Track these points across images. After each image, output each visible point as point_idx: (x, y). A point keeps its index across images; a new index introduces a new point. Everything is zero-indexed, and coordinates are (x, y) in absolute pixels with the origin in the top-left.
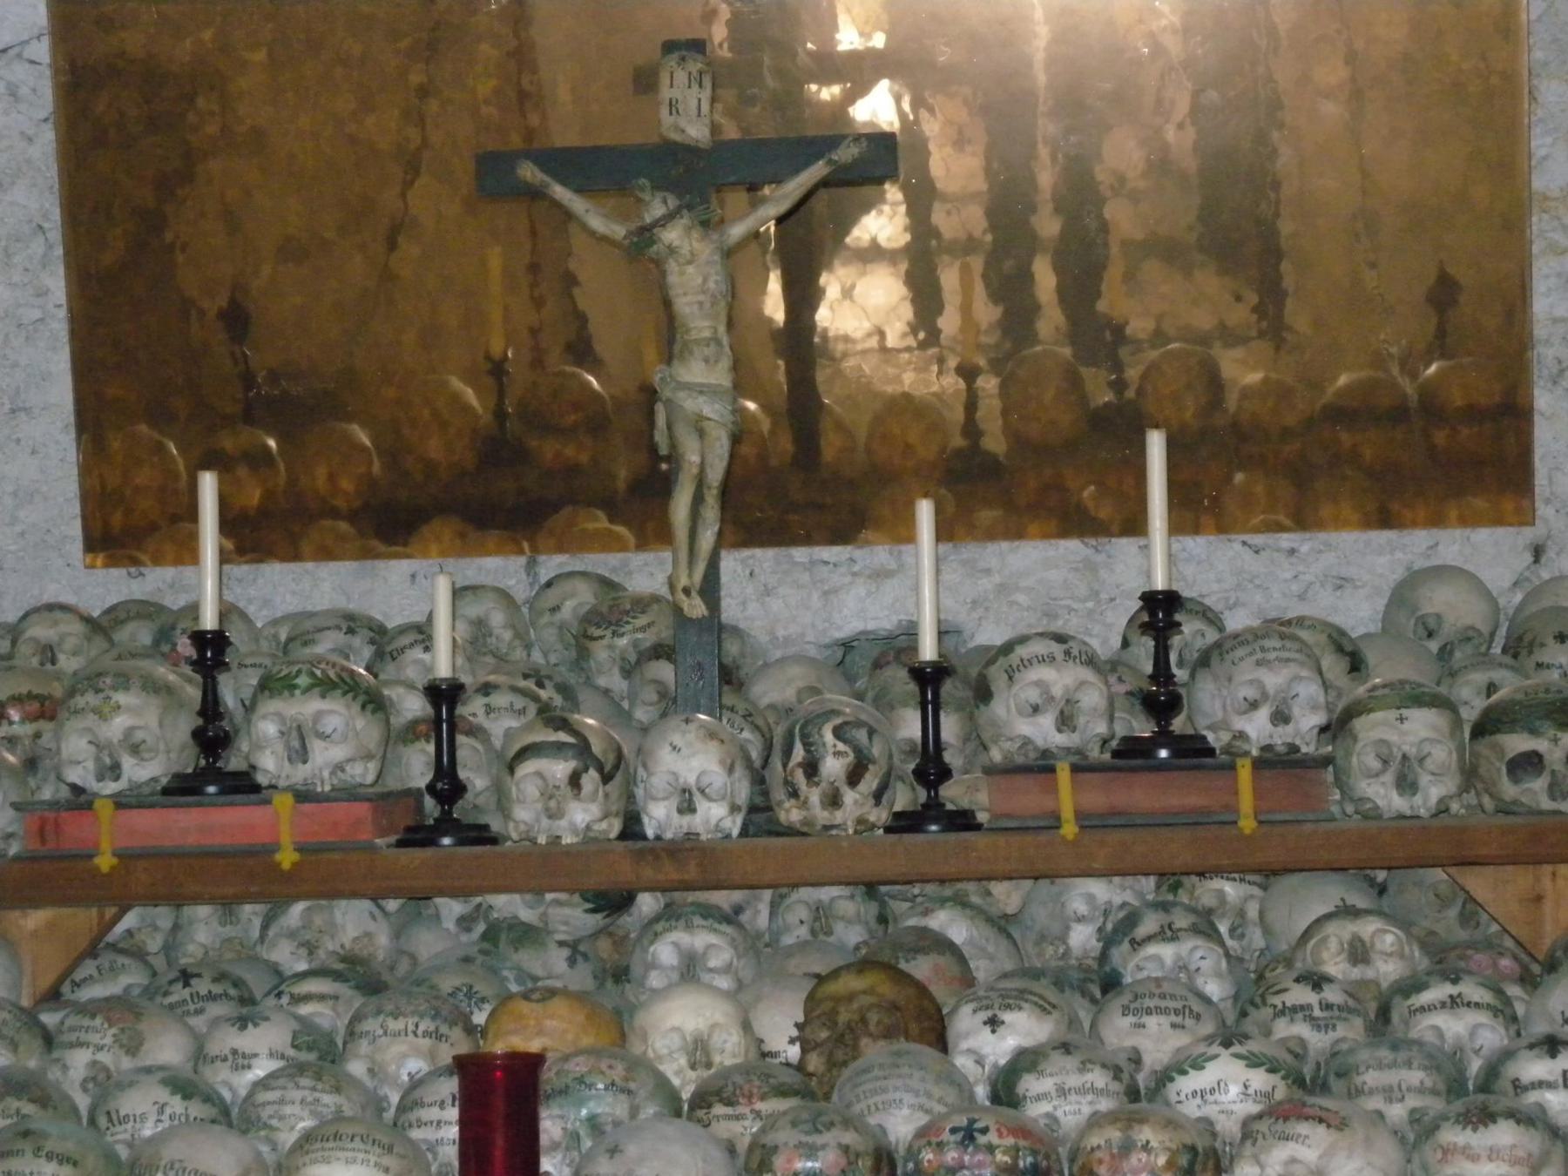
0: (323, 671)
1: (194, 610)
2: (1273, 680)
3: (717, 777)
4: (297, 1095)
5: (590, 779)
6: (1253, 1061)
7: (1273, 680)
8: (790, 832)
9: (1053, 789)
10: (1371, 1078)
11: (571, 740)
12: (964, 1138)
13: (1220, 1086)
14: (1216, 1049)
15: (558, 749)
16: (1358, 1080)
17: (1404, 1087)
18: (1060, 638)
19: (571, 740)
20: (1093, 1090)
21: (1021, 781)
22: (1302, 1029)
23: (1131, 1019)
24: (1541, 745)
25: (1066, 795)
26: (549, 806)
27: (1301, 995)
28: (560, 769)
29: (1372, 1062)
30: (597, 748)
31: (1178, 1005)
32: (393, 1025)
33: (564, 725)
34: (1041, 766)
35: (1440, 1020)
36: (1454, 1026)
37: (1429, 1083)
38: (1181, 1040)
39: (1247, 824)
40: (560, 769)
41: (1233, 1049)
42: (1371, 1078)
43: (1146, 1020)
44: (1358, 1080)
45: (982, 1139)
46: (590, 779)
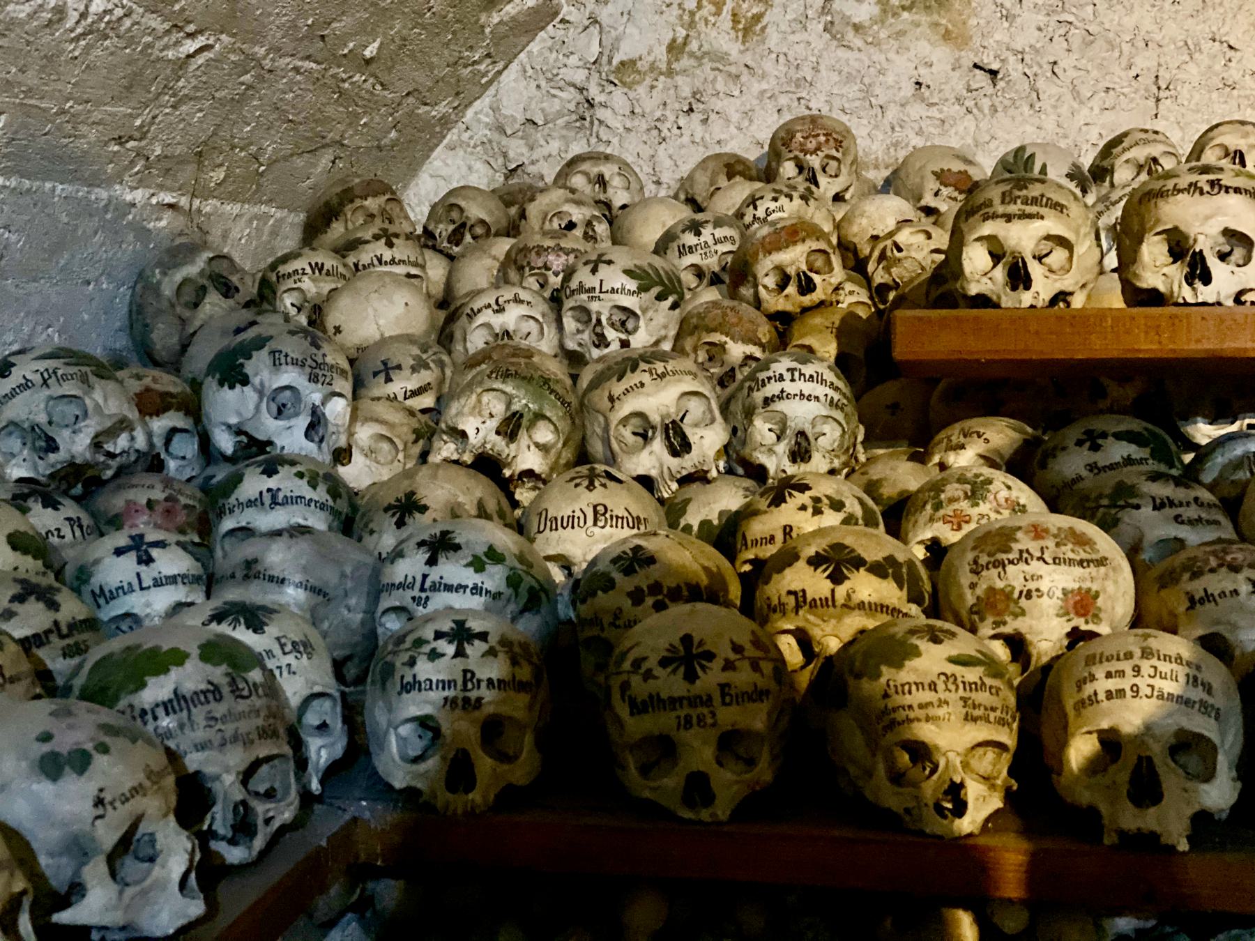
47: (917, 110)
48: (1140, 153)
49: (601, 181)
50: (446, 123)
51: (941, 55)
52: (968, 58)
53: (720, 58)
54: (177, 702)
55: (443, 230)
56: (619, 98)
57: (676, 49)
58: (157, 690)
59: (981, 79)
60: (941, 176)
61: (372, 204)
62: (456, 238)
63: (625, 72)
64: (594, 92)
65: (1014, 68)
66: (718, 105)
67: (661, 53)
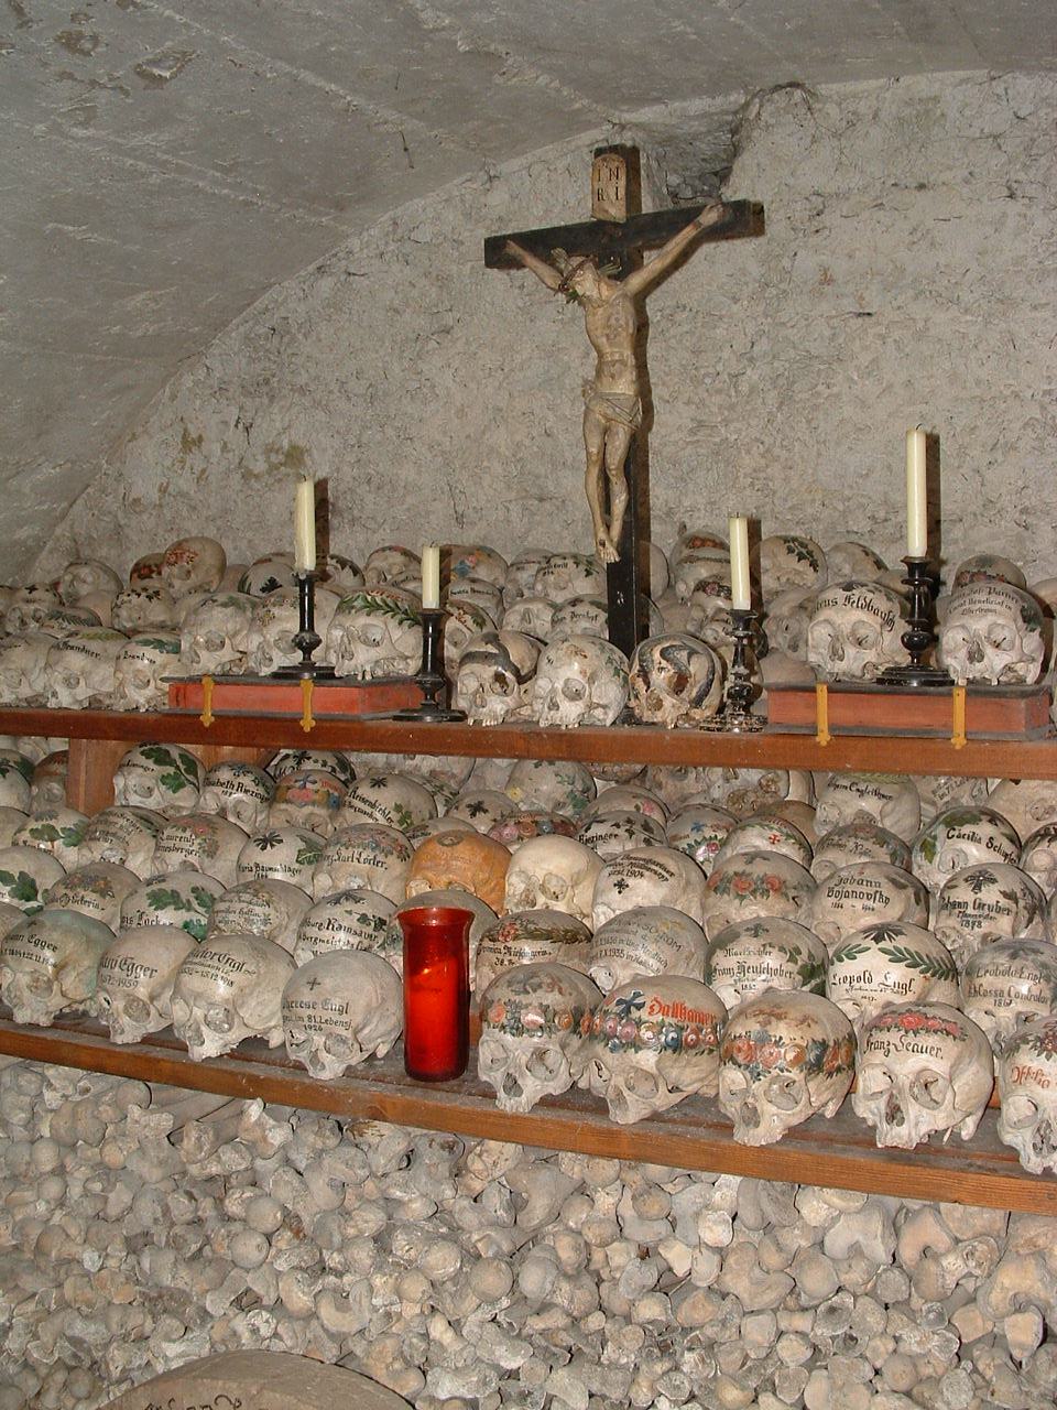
0: (373, 597)
1: (287, 557)
4: (237, 906)
6: (896, 957)
9: (814, 706)
10: (987, 981)
11: (495, 651)
12: (622, 1011)
13: (866, 977)
14: (869, 943)
16: (978, 981)
17: (1012, 994)
19: (495, 651)
20: (768, 970)
21: (790, 697)
23: (833, 900)
25: (823, 711)
29: (990, 968)
31: (871, 890)
32: (345, 853)
37: (1036, 992)
39: (959, 741)
41: (882, 945)
42: (987, 981)
43: (844, 901)
44: (978, 981)
45: (635, 1014)
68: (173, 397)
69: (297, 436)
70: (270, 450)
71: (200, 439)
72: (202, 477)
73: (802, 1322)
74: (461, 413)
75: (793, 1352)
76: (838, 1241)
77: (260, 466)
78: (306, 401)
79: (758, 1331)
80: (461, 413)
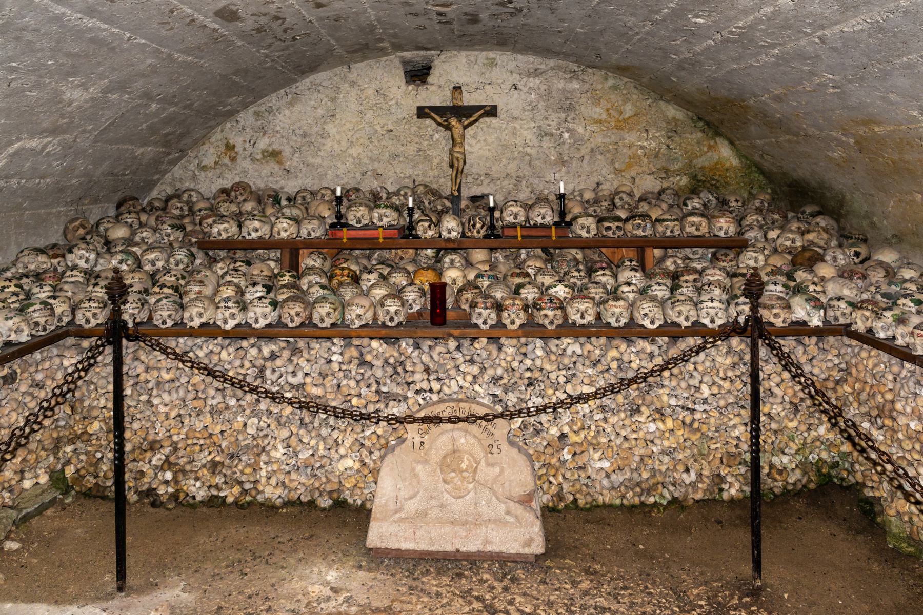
2: (543, 211)
3: (456, 227)
5: (432, 226)
7: (543, 211)
8: (468, 237)
15: (426, 221)
18: (515, 201)
22: (576, 281)
24: (611, 225)
26: (425, 231)
27: (576, 274)
28: (427, 224)
30: (434, 219)
33: (427, 215)
34: (514, 226)
35: (601, 278)
36: (604, 279)
38: (552, 281)
40: (427, 224)
46: (432, 226)
47: (271, 179)
48: (301, 195)
49: (190, 196)
50: (159, 180)
51: (276, 167)
52: (283, 167)
53: (226, 165)
54: (35, 311)
55: (148, 208)
56: (203, 174)
57: (216, 163)
58: (31, 309)
59: (285, 172)
60: (269, 196)
61: (131, 203)
62: (151, 210)
63: (204, 168)
64: (197, 173)
65: (293, 171)
66: (227, 176)
67: (212, 164)
68: (222, 131)
69: (276, 147)
70: (263, 152)
71: (234, 146)
72: (233, 159)
73: (564, 372)
74: (339, 142)
75: (562, 380)
76: (569, 351)
77: (259, 157)
78: (279, 136)
79: (553, 376)
80: (339, 142)
